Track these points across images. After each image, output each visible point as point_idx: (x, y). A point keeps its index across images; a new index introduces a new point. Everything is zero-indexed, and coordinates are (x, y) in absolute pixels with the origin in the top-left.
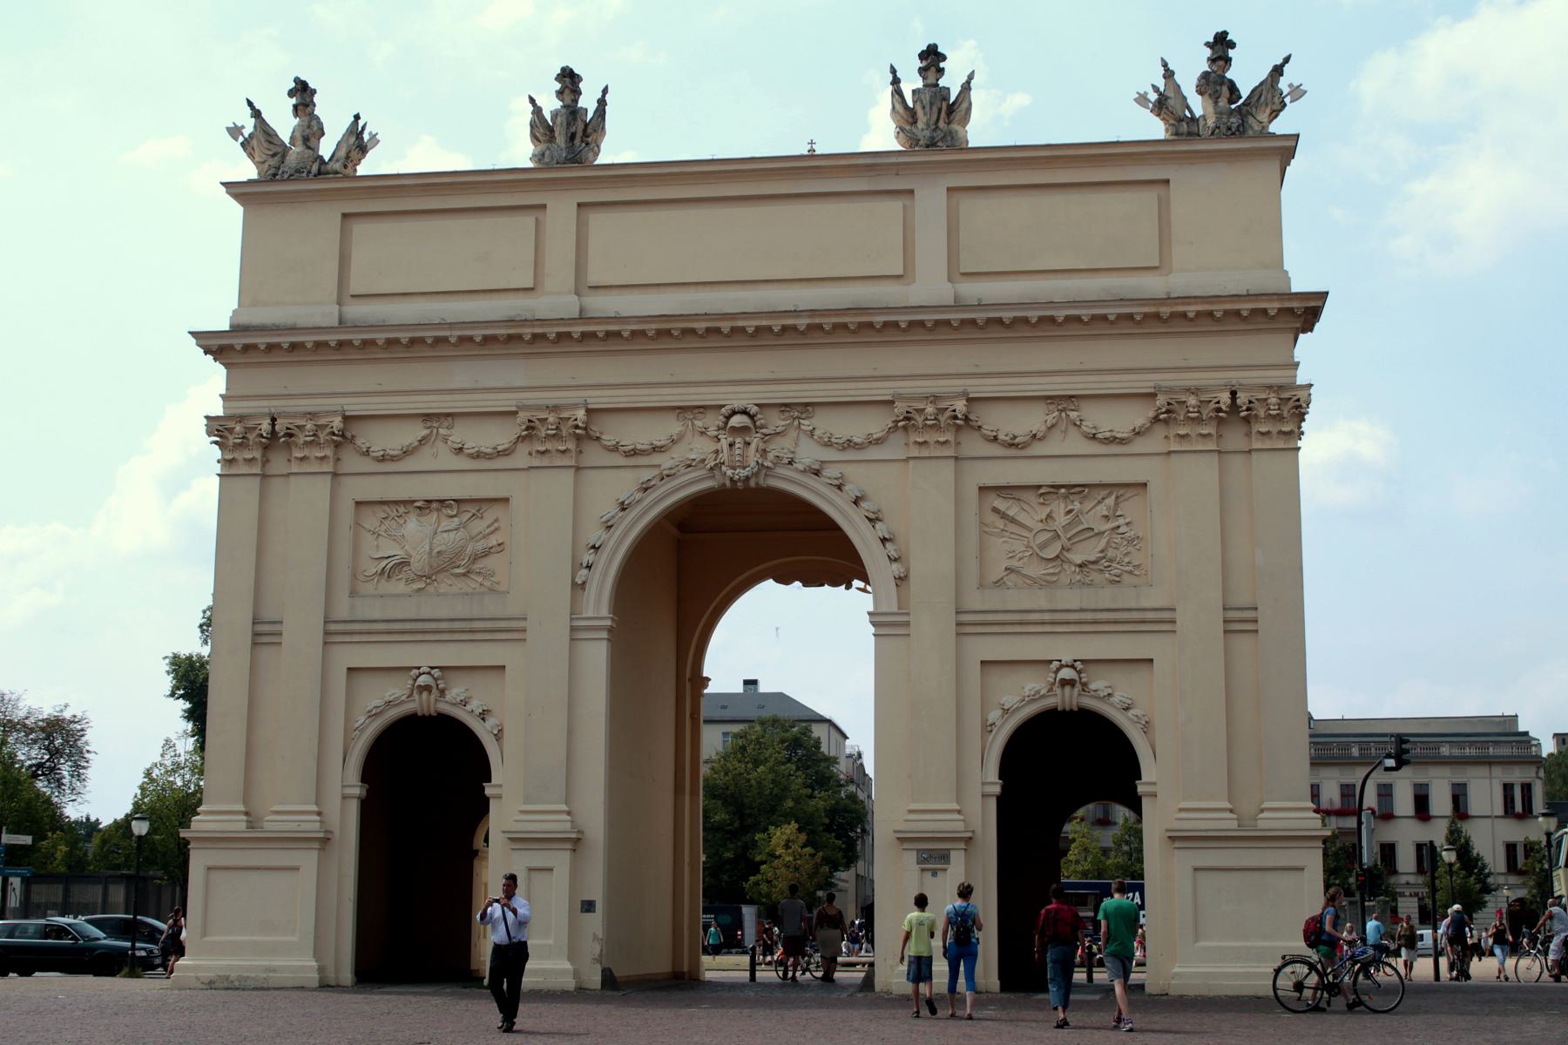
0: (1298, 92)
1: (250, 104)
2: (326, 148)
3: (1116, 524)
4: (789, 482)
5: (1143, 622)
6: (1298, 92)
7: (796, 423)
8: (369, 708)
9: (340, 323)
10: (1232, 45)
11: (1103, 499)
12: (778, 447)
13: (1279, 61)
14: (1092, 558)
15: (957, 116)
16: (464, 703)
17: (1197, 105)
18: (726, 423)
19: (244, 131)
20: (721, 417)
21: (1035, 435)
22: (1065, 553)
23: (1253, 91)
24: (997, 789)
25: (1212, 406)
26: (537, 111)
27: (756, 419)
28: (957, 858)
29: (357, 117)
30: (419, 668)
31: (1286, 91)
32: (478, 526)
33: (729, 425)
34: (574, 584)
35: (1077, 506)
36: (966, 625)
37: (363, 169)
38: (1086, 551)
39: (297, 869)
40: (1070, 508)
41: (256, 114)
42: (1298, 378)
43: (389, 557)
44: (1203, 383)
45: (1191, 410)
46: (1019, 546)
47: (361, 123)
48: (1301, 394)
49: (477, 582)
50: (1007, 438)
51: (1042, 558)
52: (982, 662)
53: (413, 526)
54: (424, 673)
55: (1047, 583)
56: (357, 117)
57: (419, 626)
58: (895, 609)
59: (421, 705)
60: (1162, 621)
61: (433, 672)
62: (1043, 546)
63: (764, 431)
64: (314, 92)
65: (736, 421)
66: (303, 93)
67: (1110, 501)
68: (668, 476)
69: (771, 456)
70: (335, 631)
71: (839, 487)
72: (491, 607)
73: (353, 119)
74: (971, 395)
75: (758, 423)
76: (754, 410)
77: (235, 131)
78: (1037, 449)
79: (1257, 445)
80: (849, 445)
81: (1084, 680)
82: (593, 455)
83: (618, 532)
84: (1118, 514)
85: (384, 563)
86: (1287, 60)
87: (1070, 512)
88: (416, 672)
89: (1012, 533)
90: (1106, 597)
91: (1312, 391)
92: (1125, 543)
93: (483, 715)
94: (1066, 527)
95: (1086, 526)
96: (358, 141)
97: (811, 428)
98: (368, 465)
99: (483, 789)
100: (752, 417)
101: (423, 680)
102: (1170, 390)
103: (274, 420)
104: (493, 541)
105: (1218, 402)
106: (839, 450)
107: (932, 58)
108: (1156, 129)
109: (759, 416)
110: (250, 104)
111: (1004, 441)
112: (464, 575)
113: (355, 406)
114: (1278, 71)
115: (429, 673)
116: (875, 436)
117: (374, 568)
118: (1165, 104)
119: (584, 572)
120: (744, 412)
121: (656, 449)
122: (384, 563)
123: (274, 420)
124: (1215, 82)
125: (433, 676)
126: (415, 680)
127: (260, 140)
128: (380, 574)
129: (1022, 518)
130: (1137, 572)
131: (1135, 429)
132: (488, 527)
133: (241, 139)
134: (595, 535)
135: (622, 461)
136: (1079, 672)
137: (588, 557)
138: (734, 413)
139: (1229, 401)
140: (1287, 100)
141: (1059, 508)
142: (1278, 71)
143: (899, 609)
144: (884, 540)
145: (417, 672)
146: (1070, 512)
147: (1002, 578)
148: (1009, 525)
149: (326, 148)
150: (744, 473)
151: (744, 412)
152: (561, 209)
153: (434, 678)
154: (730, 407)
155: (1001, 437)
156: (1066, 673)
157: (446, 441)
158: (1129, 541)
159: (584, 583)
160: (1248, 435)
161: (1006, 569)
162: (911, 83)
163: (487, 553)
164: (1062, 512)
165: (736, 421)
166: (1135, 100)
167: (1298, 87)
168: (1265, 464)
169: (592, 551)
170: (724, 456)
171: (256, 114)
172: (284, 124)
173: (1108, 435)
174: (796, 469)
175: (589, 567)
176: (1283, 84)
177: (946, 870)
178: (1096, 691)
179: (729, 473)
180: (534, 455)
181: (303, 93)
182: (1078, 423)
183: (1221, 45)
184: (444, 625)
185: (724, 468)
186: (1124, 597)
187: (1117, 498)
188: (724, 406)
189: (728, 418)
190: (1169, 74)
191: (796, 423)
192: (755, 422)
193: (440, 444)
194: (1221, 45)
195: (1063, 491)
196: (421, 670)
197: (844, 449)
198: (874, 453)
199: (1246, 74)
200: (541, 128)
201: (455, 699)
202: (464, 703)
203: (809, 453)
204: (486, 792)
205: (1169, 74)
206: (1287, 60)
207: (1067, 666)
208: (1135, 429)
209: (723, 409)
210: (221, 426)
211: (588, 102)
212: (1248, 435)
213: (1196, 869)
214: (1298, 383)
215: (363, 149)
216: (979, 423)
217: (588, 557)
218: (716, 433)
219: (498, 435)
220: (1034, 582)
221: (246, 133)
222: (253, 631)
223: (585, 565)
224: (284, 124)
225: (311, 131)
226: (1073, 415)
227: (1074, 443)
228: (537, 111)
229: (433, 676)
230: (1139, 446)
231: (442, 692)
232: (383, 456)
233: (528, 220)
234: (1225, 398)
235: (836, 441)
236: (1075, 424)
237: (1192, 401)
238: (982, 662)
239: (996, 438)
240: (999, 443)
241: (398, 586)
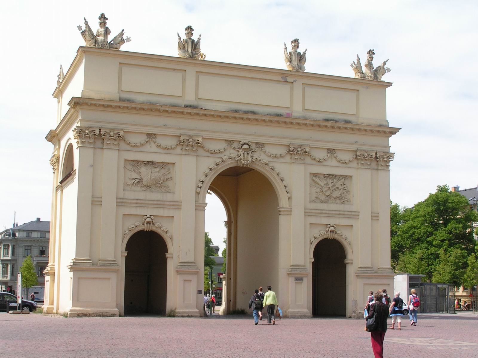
0: (389, 70)
1: (85, 19)
2: (110, 38)
3: (344, 187)
4: (258, 167)
5: (351, 215)
6: (389, 70)
7: (261, 149)
8: (129, 228)
9: (120, 100)
10: (374, 54)
11: (341, 179)
12: (256, 155)
13: (386, 61)
14: (338, 196)
15: (303, 61)
16: (160, 228)
17: (364, 69)
18: (241, 147)
19: (82, 28)
20: (240, 145)
21: (325, 159)
22: (331, 194)
23: (377, 68)
24: (313, 260)
25: (370, 156)
26: (180, 39)
27: (250, 146)
28: (305, 280)
29: (123, 31)
30: (147, 215)
31: (386, 69)
32: (163, 171)
33: (242, 148)
34: (196, 192)
35: (335, 181)
36: (308, 213)
37: (124, 48)
38: (336, 194)
39: (109, 279)
40: (333, 181)
41: (86, 23)
42: (390, 151)
43: (136, 179)
44: (369, 149)
45: (366, 157)
46: (318, 190)
47: (123, 32)
48: (391, 155)
49: (164, 189)
50: (318, 159)
51: (325, 194)
52: (310, 224)
53: (144, 170)
54: (149, 217)
55: (326, 202)
56: (123, 31)
57: (147, 202)
58: (288, 207)
59: (147, 228)
60: (354, 215)
61: (152, 217)
62: (326, 191)
63: (252, 150)
64: (107, 19)
65: (246, 147)
66: (103, 18)
67: (343, 180)
68: (224, 161)
69: (254, 158)
70: (120, 203)
71: (273, 169)
72: (169, 197)
73: (121, 31)
74: (311, 146)
75: (251, 148)
76: (250, 144)
77: (80, 28)
78: (325, 163)
79: (380, 168)
80: (276, 157)
81: (336, 230)
82: (201, 152)
83: (209, 177)
84: (344, 184)
85: (134, 181)
86: (387, 61)
87: (332, 183)
88: (145, 217)
89: (317, 187)
90: (340, 207)
91: (395, 155)
92: (346, 192)
93: (166, 232)
94: (332, 186)
95: (337, 187)
96: (120, 39)
97: (265, 151)
98: (128, 147)
99: (165, 255)
100: (249, 146)
101: (148, 219)
102: (361, 150)
103: (100, 130)
104: (169, 176)
105: (372, 155)
106: (273, 158)
107: (296, 42)
108: (351, 74)
109: (251, 146)
110: (85, 19)
111: (317, 160)
112: (160, 187)
113: (128, 128)
114: (385, 63)
115: (150, 217)
116: (283, 155)
117: (130, 182)
118: (357, 68)
119: (199, 189)
120: (247, 144)
121: (220, 152)
122: (134, 181)
123: (100, 130)
124: (369, 65)
125: (151, 218)
126: (145, 219)
127: (87, 32)
128: (132, 184)
129: (320, 183)
130: (348, 201)
131: (350, 160)
132: (167, 172)
133: (81, 31)
134: (203, 178)
135: (210, 155)
136: (335, 228)
137: (200, 184)
138: (244, 144)
139: (375, 156)
140: (386, 71)
141: (330, 181)
142: (385, 63)
143: (289, 207)
144: (285, 187)
145: (145, 217)
146: (332, 183)
147: (314, 200)
148: (317, 184)
149: (110, 38)
150: (248, 162)
151: (247, 144)
152: (191, 72)
153: (152, 219)
154: (243, 142)
155: (317, 159)
156: (332, 228)
157: (155, 143)
158: (346, 192)
159: (199, 192)
160: (377, 165)
161: (316, 197)
162: (290, 49)
163: (167, 180)
164: (330, 182)
165: (246, 147)
166: (351, 65)
167: (389, 69)
168: (382, 173)
169: (201, 182)
170: (242, 157)
171: (86, 23)
172: (95, 27)
173: (343, 161)
174: (261, 163)
175: (201, 188)
176: (385, 67)
177: (302, 283)
178: (339, 234)
179: (243, 162)
180: (184, 150)
181: (103, 18)
182: (336, 157)
183: (371, 53)
184: (155, 202)
185: (241, 161)
186: (347, 207)
187: (344, 180)
188: (241, 141)
189: (242, 145)
190: (359, 60)
191: (261, 149)
192: (250, 147)
193: (152, 144)
194: (371, 53)
195: (331, 176)
196: (148, 216)
197: (274, 158)
198: (281, 160)
199: (376, 64)
200: (182, 46)
201: (158, 226)
202: (160, 228)
203: (265, 159)
204: (166, 256)
205: (359, 60)
206: (387, 61)
207: (332, 226)
208: (350, 160)
209: (241, 142)
210: (81, 130)
211: (195, 38)
212: (377, 165)
213: (364, 284)
214: (390, 152)
215: (123, 41)
216: (311, 154)
217: (200, 184)
218: (238, 149)
219: (172, 142)
220: (322, 202)
221: (84, 28)
222: (116, 201)
223: (200, 187)
224: (95, 27)
225: (107, 31)
226: (335, 155)
227: (334, 163)
228: (180, 39)
229: (151, 218)
230: (351, 165)
231: (154, 224)
232: (135, 145)
233: (179, 75)
234: (374, 154)
235: (272, 155)
236: (335, 157)
237: (366, 155)
238: (310, 224)
239: (315, 159)
240: (315, 161)
241: (138, 188)
